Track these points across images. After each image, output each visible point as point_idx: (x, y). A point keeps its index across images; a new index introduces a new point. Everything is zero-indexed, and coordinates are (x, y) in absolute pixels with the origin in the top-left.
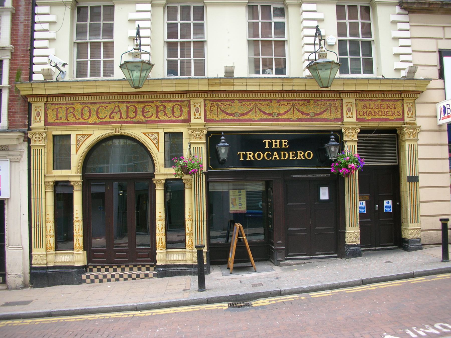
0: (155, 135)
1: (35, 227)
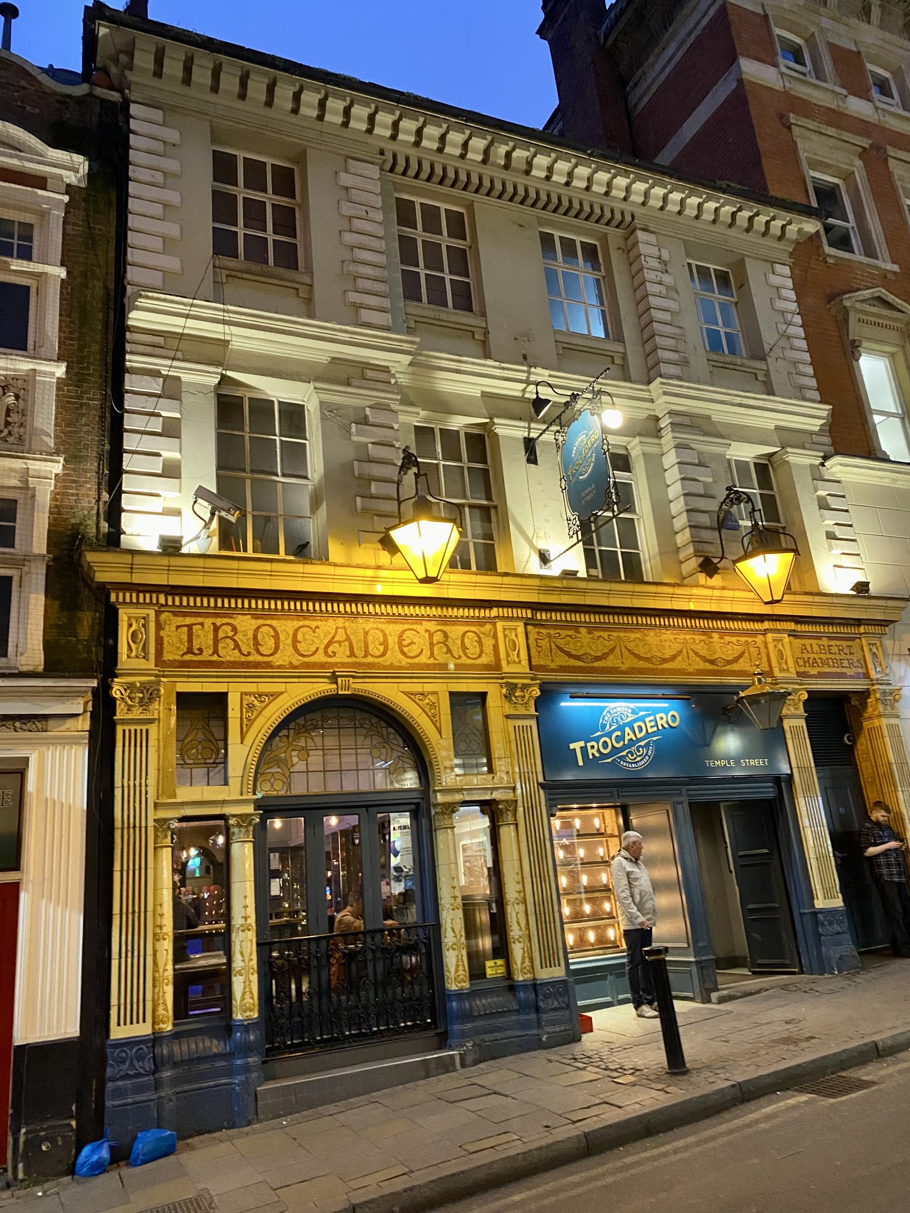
0: (430, 697)
1: (123, 955)
